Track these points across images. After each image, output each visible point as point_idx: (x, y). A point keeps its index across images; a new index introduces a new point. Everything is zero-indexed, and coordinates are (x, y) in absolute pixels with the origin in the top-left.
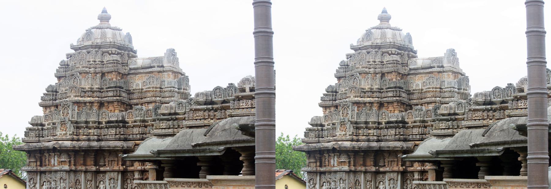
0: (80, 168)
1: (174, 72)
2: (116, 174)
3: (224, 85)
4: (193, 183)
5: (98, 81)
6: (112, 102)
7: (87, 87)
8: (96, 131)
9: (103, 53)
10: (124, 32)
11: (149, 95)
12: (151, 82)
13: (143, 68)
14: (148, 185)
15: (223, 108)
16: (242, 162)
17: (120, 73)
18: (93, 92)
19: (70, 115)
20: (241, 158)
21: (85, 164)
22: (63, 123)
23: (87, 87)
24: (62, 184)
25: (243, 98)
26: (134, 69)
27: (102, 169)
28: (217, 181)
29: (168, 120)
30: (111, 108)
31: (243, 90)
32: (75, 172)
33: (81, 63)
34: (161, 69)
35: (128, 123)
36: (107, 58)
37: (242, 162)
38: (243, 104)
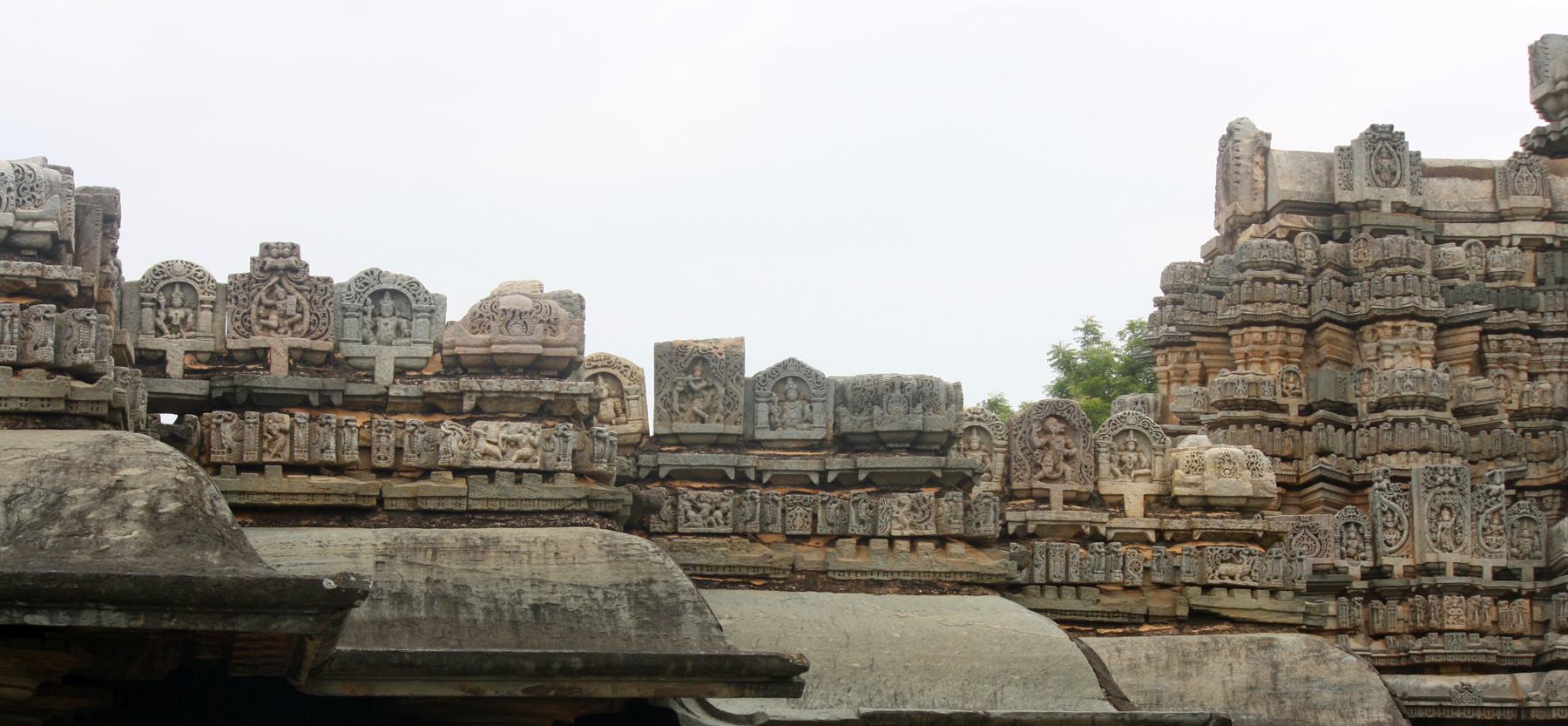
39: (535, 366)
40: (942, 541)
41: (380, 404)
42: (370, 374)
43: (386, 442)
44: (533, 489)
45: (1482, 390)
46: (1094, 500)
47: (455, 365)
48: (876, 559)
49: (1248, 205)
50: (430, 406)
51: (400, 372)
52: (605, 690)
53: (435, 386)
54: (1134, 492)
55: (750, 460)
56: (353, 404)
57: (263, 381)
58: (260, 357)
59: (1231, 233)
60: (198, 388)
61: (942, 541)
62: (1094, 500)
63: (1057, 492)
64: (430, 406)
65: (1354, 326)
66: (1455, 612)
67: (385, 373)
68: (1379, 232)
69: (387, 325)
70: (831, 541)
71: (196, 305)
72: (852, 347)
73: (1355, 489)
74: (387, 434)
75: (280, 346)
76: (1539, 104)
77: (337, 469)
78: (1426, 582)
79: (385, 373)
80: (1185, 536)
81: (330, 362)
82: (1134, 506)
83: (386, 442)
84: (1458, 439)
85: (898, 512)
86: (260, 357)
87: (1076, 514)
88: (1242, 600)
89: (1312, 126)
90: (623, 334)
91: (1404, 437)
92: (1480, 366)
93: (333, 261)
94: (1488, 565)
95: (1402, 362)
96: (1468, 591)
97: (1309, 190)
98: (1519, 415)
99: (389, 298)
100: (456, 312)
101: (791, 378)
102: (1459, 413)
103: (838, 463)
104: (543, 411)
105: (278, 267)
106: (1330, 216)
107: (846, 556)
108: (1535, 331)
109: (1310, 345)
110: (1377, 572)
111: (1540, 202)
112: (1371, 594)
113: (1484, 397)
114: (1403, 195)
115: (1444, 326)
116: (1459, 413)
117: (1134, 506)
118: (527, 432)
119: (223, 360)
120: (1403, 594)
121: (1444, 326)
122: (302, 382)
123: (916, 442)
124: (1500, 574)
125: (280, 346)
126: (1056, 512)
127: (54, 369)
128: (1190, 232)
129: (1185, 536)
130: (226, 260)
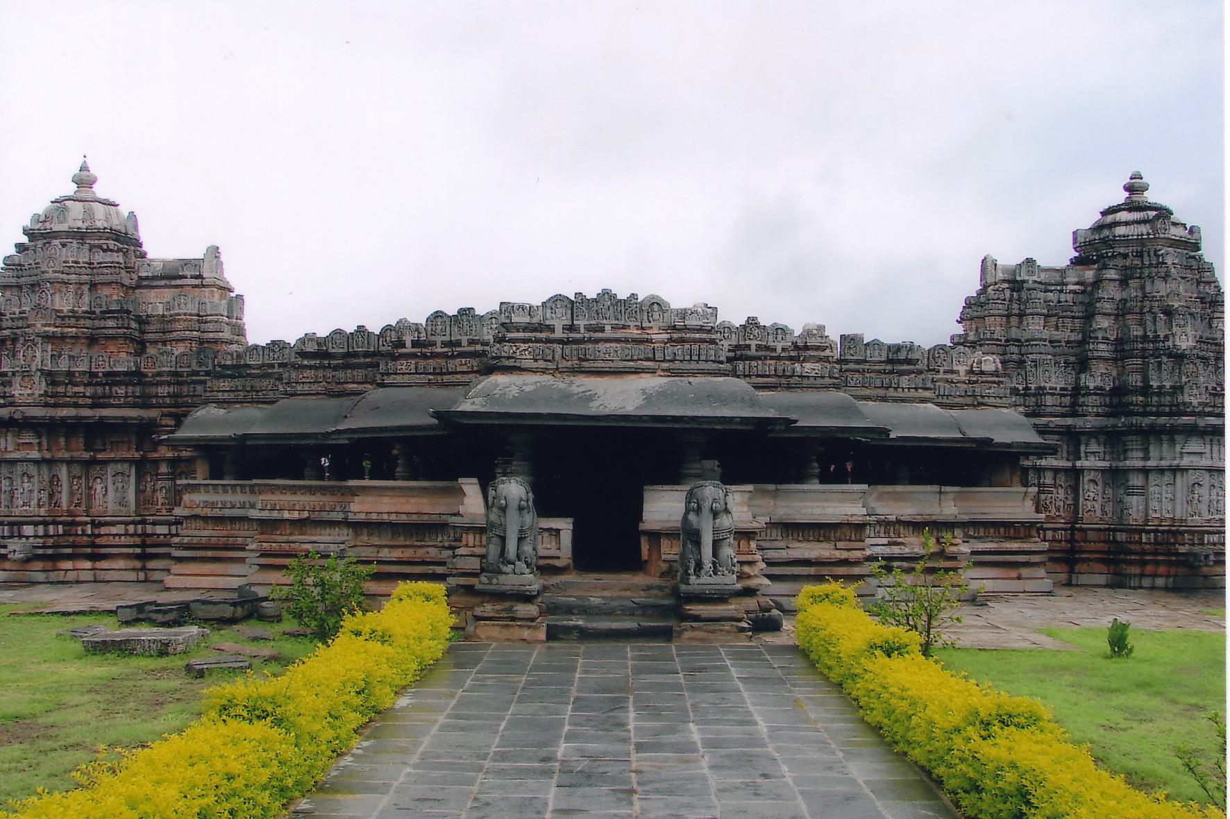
0: (60, 455)
1: (222, 288)
2: (126, 466)
3: (350, 328)
4: (300, 487)
5: (86, 299)
6: (114, 338)
7: (65, 309)
8: (89, 391)
9: (92, 247)
10: (124, 210)
11: (178, 326)
12: (182, 306)
13: (162, 278)
14: (202, 489)
15: (346, 367)
16: (396, 458)
17: (123, 285)
18: (78, 319)
19: (38, 359)
20: (395, 452)
21: (68, 450)
22: (26, 374)
23: (65, 309)
24: (26, 485)
25: (402, 356)
26: (147, 278)
27: (100, 456)
28: (364, 488)
29: (232, 377)
30: (112, 348)
31: (401, 344)
32: (50, 462)
33: (51, 264)
34: (197, 282)
35: (146, 376)
36: (100, 257)
37: (396, 458)
38: (402, 365)
39: (818, 348)
40: (916, 389)
41: (779, 358)
42: (775, 350)
43: (780, 368)
44: (819, 381)
45: (1057, 335)
46: (952, 372)
47: (796, 347)
48: (900, 394)
49: (990, 280)
50: (791, 358)
51: (783, 350)
52: (840, 435)
53: (793, 354)
54: (962, 369)
55: (867, 367)
56: (772, 358)
57: (749, 353)
58: (748, 347)
59: (985, 287)
60: (732, 354)
61: (916, 389)
62: (952, 372)
63: (941, 369)
64: (791, 358)
65: (1021, 315)
66: (1049, 400)
67: (779, 350)
68: (1029, 289)
69: (779, 337)
70: (887, 388)
71: (731, 332)
72: (891, 336)
73: (1021, 363)
74: (781, 365)
75: (753, 344)
76: (1075, 249)
77: (768, 376)
78: (1041, 392)
79: (779, 350)
80: (977, 382)
81: (767, 348)
82: (962, 373)
83: (780, 368)
84: (1051, 350)
85: (904, 382)
86: (748, 347)
87: (949, 376)
88: (992, 400)
89: (1009, 257)
90: (834, 335)
91: (1035, 349)
92: (1057, 328)
93: (765, 321)
94: (1059, 387)
95: (1035, 327)
96: (1053, 394)
97: (1007, 277)
98: (1068, 342)
99: (781, 330)
100: (796, 334)
101: (875, 344)
102: (1051, 342)
103: (889, 367)
104: (820, 360)
105: (752, 323)
106: (1015, 284)
107: (891, 393)
108: (1073, 317)
109: (1008, 322)
110: (1027, 388)
111: (1076, 280)
112: (1025, 395)
113: (1057, 338)
114: (1035, 278)
115: (1046, 316)
116: (1051, 342)
117: (962, 373)
118: (818, 366)
119: (738, 347)
120: (1034, 395)
121: (1046, 316)
122: (760, 353)
123: (909, 361)
124: (1062, 389)
125: (753, 344)
126: (941, 376)
127: (714, 361)
128: (972, 286)
129: (977, 382)
130: (738, 321)
